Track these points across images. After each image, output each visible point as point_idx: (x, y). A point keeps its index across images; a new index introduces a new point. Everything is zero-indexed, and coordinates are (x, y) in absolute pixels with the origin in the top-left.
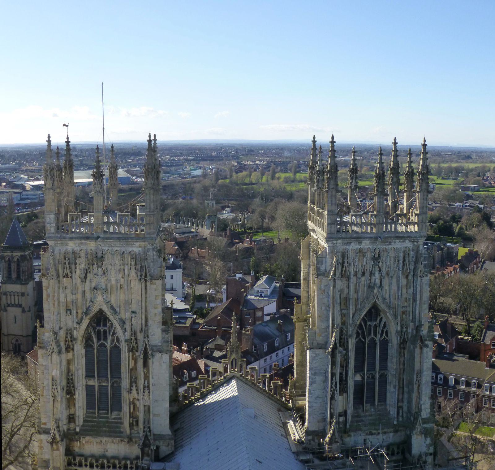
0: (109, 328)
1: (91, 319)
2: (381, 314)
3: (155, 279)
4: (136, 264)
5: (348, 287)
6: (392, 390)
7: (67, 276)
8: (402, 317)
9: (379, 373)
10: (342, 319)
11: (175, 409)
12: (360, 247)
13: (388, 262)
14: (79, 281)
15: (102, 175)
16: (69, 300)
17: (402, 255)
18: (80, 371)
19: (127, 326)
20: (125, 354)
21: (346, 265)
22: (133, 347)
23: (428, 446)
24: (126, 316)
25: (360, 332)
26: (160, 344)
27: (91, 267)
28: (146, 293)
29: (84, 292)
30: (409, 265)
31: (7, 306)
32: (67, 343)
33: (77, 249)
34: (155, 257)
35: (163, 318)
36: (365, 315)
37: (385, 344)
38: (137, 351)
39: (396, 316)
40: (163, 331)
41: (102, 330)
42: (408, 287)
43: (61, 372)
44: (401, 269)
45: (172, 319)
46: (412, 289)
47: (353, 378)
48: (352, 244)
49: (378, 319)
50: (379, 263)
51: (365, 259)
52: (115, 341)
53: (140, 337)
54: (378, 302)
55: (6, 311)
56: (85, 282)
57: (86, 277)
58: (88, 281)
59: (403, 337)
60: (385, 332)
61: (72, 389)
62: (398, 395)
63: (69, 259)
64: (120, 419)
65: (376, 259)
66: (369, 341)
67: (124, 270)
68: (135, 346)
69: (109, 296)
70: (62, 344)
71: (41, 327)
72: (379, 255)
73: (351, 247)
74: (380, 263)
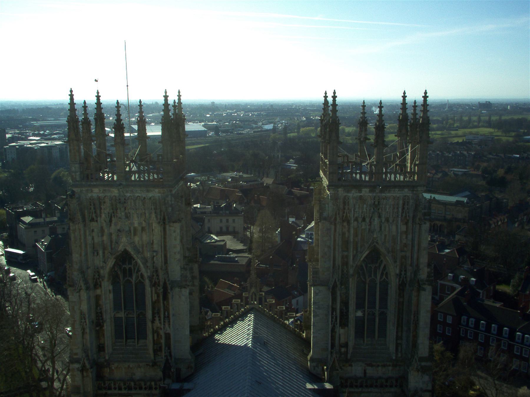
0: (134, 265)
3: (174, 222)
4: (155, 209)
5: (349, 231)
7: (92, 220)
9: (379, 311)
14: (104, 225)
17: (401, 202)
19: (149, 264)
20: (148, 289)
22: (155, 282)
24: (148, 255)
26: (179, 279)
29: (111, 234)
30: (408, 213)
34: (173, 202)
38: (159, 286)
41: (127, 268)
44: (400, 216)
47: (355, 314)
48: (353, 192)
50: (379, 209)
51: (365, 206)
52: (140, 278)
53: (161, 273)
56: (111, 225)
57: (111, 221)
58: (113, 225)
59: (401, 279)
61: (101, 321)
62: (397, 332)
63: (94, 205)
65: (376, 205)
67: (145, 214)
68: (157, 281)
72: (379, 202)
74: (380, 210)
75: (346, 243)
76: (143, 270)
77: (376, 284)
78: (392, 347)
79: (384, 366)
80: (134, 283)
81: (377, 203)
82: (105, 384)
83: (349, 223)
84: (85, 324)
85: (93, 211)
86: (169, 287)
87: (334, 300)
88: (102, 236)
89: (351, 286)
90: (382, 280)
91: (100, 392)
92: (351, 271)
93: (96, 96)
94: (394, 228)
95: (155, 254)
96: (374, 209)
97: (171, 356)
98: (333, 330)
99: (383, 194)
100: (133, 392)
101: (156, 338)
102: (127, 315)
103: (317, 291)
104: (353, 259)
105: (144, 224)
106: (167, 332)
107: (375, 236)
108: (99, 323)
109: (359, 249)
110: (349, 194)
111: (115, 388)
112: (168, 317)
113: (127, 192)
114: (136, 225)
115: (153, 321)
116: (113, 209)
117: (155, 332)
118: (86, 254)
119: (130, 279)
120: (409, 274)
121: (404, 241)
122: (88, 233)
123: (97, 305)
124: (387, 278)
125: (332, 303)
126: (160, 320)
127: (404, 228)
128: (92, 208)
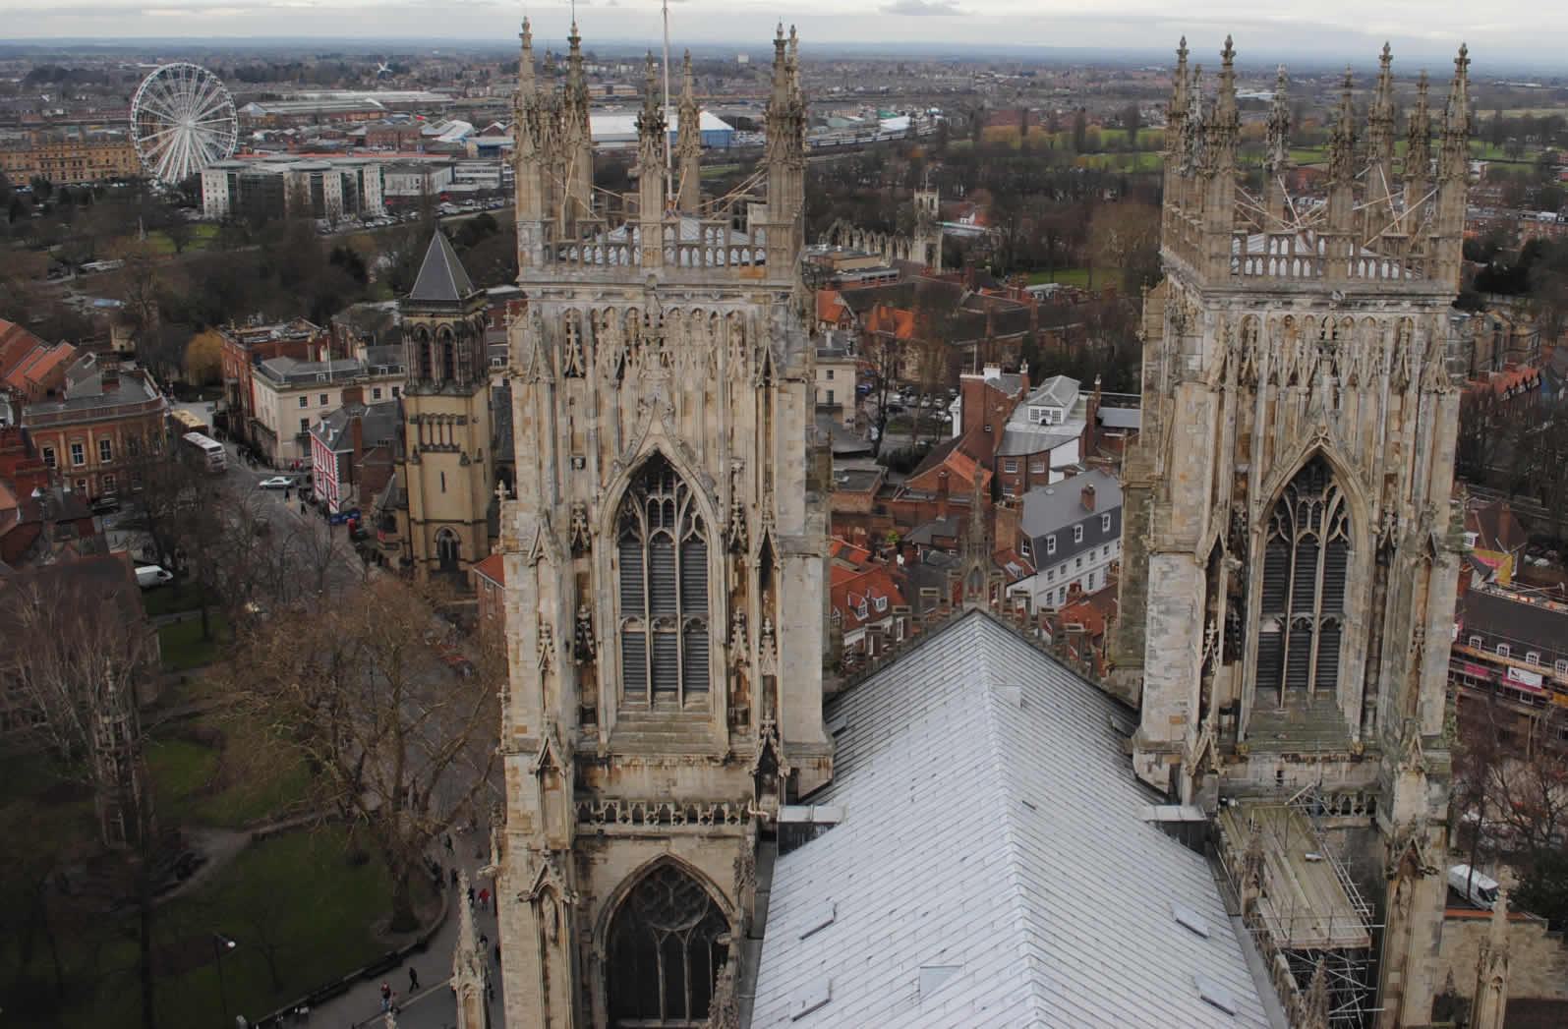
1: (633, 476)
2: (1334, 477)
3: (790, 380)
4: (743, 343)
5: (1254, 409)
6: (1353, 661)
7: (572, 373)
8: (1386, 488)
10: (1237, 486)
11: (836, 683)
12: (1287, 313)
13: (1357, 351)
14: (604, 384)
15: (661, 126)
16: (578, 430)
17: (1390, 336)
18: (608, 602)
20: (716, 557)
22: (737, 541)
23: (1434, 804)
25: (1279, 518)
26: (801, 534)
27: (633, 351)
28: (768, 413)
30: (1410, 361)
31: (422, 451)
32: (575, 534)
33: (600, 306)
34: (789, 328)
35: (808, 475)
36: (1293, 479)
37: (1338, 550)
38: (746, 551)
40: (809, 502)
41: (661, 503)
42: (1404, 417)
43: (563, 605)
45: (829, 478)
46: (1413, 422)
47: (1259, 626)
48: (1269, 306)
49: (1326, 491)
50: (1333, 353)
51: (1298, 343)
52: (693, 529)
53: (755, 520)
54: (1326, 448)
55: (420, 462)
56: (620, 388)
57: (620, 376)
58: (626, 385)
59: (1385, 536)
61: (590, 643)
62: (1366, 675)
63: (578, 331)
64: (705, 709)
66: (1301, 541)
68: (742, 537)
69: (678, 420)
70: (563, 537)
71: (508, 497)
72: (1334, 334)
73: (1265, 313)
74: (1337, 356)
76: (703, 507)
77: (1318, 548)
78: (1352, 714)
79: (1328, 760)
80: (677, 542)
81: (1329, 336)
82: (597, 807)
83: (1254, 388)
84: (549, 649)
85: (576, 347)
86: (776, 550)
87: (1212, 589)
88: (597, 414)
89: (1253, 554)
90: (1332, 538)
91: (586, 828)
92: (1256, 512)
93: (570, 39)
94: (1372, 399)
95: (737, 466)
96: (1321, 351)
97: (777, 736)
98: (1206, 670)
99: (1347, 314)
100: (672, 828)
101: (733, 689)
102: (656, 626)
103: (1165, 568)
104: (1263, 482)
105: (710, 386)
106: (768, 673)
107: (1322, 423)
108: (583, 654)
109: (1278, 456)
112: (773, 633)
114: (689, 387)
115: (727, 645)
116: (627, 343)
117: (735, 672)
119: (666, 530)
120: (1403, 523)
121: (1394, 439)
122: (559, 409)
123: (580, 600)
124: (1346, 533)
128: (573, 341)
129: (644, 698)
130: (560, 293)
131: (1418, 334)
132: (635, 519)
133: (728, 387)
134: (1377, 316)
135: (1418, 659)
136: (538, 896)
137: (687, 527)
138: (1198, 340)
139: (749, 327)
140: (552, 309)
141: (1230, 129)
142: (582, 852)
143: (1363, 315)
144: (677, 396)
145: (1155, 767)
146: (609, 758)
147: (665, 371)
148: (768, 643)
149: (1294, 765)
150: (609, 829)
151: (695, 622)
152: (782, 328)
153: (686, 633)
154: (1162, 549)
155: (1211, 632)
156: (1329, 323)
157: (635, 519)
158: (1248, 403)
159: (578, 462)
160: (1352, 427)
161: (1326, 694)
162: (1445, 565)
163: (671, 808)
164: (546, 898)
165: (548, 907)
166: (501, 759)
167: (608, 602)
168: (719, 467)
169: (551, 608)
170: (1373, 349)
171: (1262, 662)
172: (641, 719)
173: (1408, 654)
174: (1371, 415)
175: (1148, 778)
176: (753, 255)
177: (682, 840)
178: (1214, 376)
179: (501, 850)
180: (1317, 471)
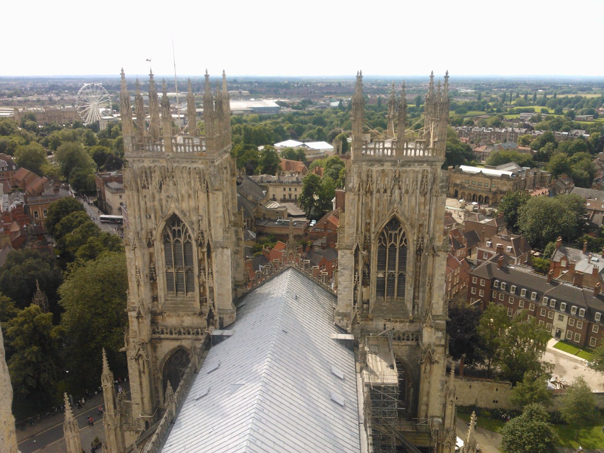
1: (167, 221)
3: (216, 190)
5: (372, 201)
6: (409, 288)
7: (144, 187)
13: (407, 181)
14: (155, 191)
16: (148, 206)
17: (420, 176)
18: (160, 262)
20: (195, 248)
21: (370, 182)
22: (201, 243)
24: (194, 218)
29: (161, 200)
33: (152, 165)
34: (216, 173)
36: (387, 225)
37: (403, 250)
39: (412, 226)
47: (375, 274)
48: (376, 166)
56: (161, 192)
57: (161, 188)
58: (162, 191)
59: (419, 245)
60: (404, 239)
61: (154, 275)
62: (414, 293)
63: (146, 173)
64: (193, 297)
65: (397, 179)
68: (202, 242)
69: (180, 203)
70: (144, 241)
74: (400, 183)
75: (369, 213)
76: (190, 232)
78: (409, 306)
79: (401, 322)
81: (397, 176)
82: (158, 329)
83: (372, 193)
85: (145, 179)
86: (212, 246)
87: (356, 262)
88: (154, 201)
89: (372, 250)
90: (401, 245)
91: (155, 336)
94: (413, 199)
95: (200, 218)
98: (355, 289)
100: (183, 336)
101: (202, 291)
103: (343, 254)
105: (191, 192)
108: (152, 279)
110: (372, 168)
111: (167, 333)
112: (212, 273)
113: (174, 162)
114: (183, 192)
115: (199, 277)
116: (162, 177)
118: (140, 217)
120: (425, 241)
123: (151, 261)
124: (406, 244)
125: (355, 265)
126: (205, 275)
127: (422, 199)
129: (174, 294)
130: (139, 161)
131: (430, 176)
132: (168, 236)
133: (196, 192)
134: (414, 169)
135: (430, 289)
136: (138, 357)
137: (185, 238)
138: (352, 178)
139: (202, 172)
140: (137, 166)
141: (361, 104)
142: (154, 343)
143: (409, 169)
144: (179, 195)
145: (341, 321)
146: (162, 313)
147: (175, 187)
148: (210, 276)
149: (389, 323)
150: (162, 336)
151: (190, 269)
152: (213, 173)
153: (187, 273)
154: (341, 248)
155: (357, 276)
156: (398, 172)
157: (168, 235)
158: (370, 199)
159: (148, 216)
160: (407, 208)
161: (401, 299)
162: (439, 256)
163: (182, 330)
164: (140, 358)
165: (141, 361)
166: (127, 313)
167: (160, 262)
168: (194, 218)
169: (139, 263)
170: (413, 181)
171: (378, 287)
172: (173, 300)
173: (427, 287)
174: (413, 203)
175: (339, 325)
176: (201, 148)
177: (186, 340)
178: (357, 189)
179: (128, 342)
180: (394, 223)
